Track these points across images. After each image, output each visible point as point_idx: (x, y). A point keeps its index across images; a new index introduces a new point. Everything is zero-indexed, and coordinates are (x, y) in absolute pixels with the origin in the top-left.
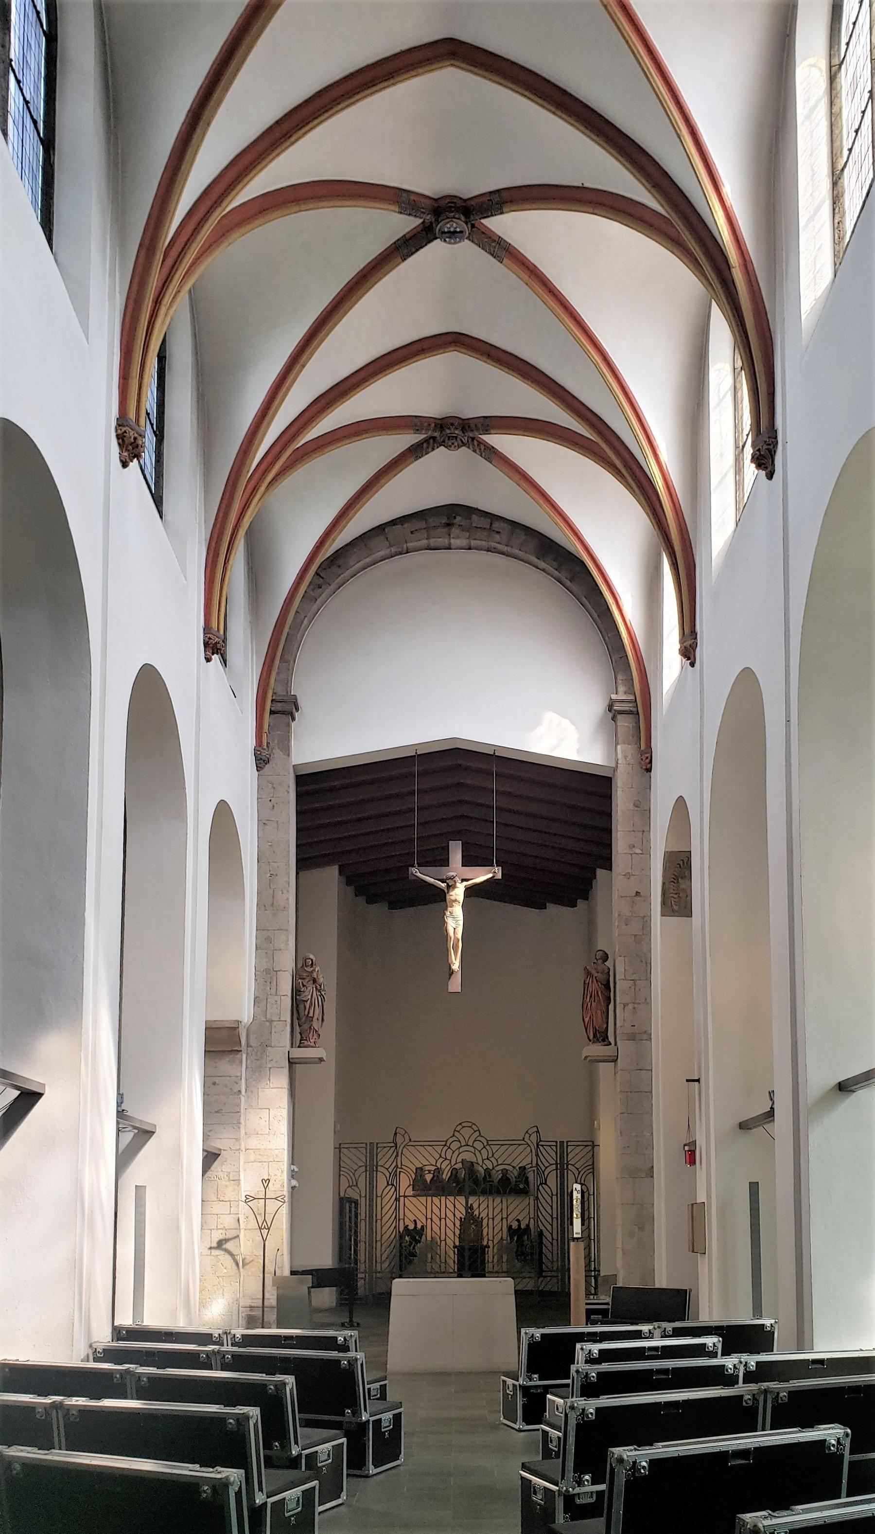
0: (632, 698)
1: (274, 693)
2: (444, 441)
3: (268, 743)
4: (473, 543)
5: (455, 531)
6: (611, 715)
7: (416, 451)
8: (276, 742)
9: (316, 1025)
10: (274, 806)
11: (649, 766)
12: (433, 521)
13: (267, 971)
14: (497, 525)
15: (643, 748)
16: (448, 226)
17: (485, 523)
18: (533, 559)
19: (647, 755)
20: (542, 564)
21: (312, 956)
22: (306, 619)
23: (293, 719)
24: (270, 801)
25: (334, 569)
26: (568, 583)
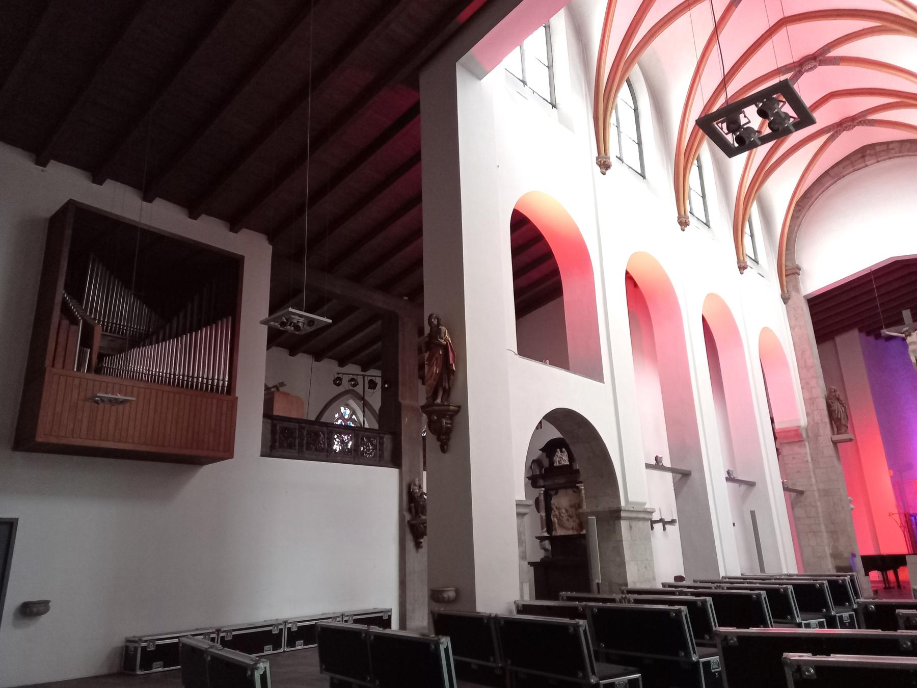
4: (879, 159)
5: (867, 158)
9: (843, 422)
12: (853, 159)
13: (810, 399)
14: (891, 146)
17: (884, 147)
21: (833, 387)
23: (799, 274)
25: (806, 200)
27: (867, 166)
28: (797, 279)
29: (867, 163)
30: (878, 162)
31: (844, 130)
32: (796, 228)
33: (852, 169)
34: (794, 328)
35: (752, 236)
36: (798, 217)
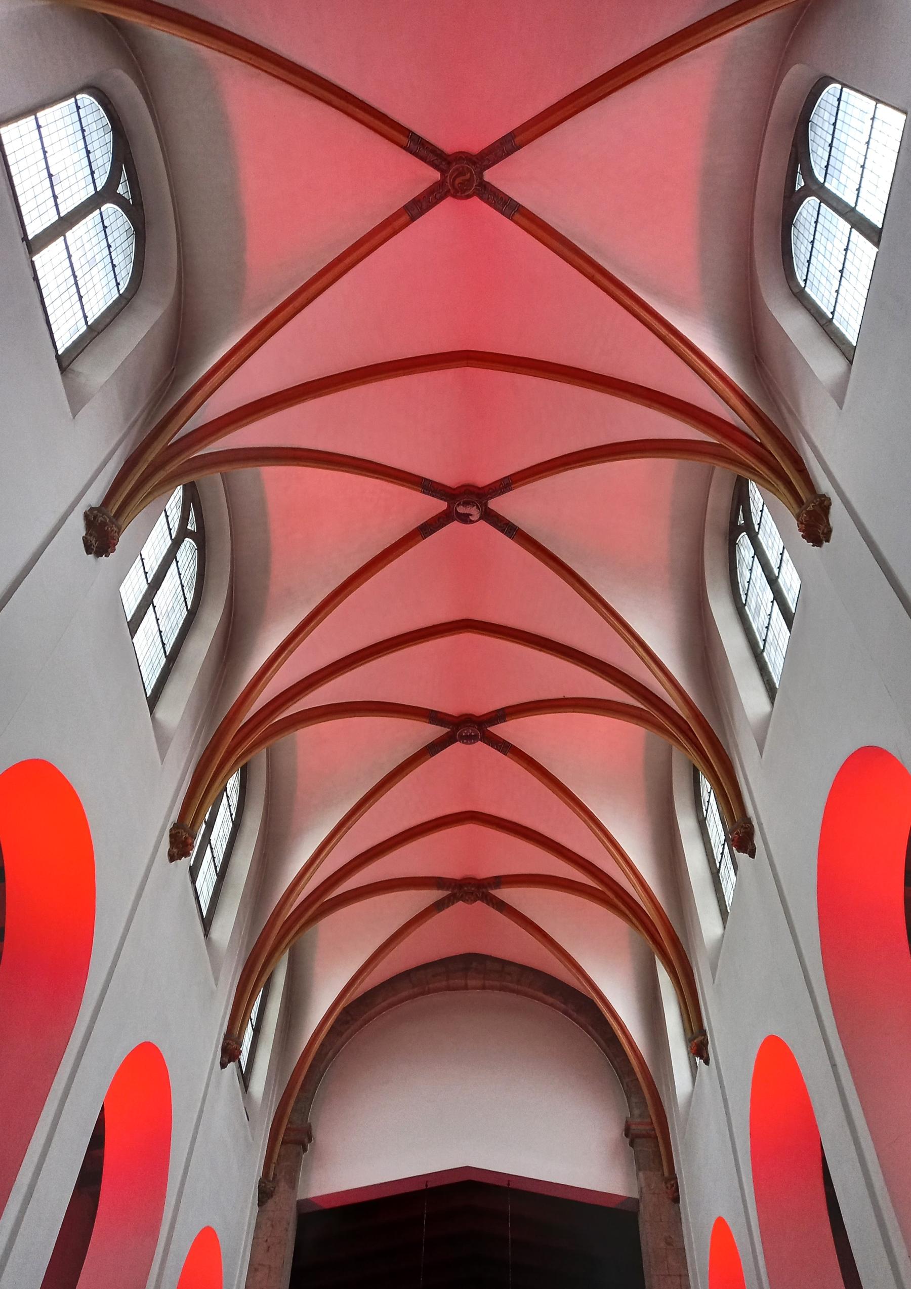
0: (648, 1120)
1: (290, 1122)
2: (462, 896)
3: (275, 1175)
4: (487, 983)
6: (628, 1140)
7: (438, 906)
8: (283, 1173)
10: (269, 1247)
11: (676, 1194)
15: (666, 1174)
16: (466, 731)
18: (541, 994)
19: (672, 1182)
20: (550, 1000)
22: (331, 1051)
23: (305, 1150)
24: (267, 1241)
26: (575, 1015)
27: (466, 988)
28: (298, 1156)
29: (472, 983)
30: (483, 988)
31: (462, 898)
32: (330, 1054)
33: (444, 983)
34: (256, 1270)
35: (257, 1031)
36: (340, 1034)
